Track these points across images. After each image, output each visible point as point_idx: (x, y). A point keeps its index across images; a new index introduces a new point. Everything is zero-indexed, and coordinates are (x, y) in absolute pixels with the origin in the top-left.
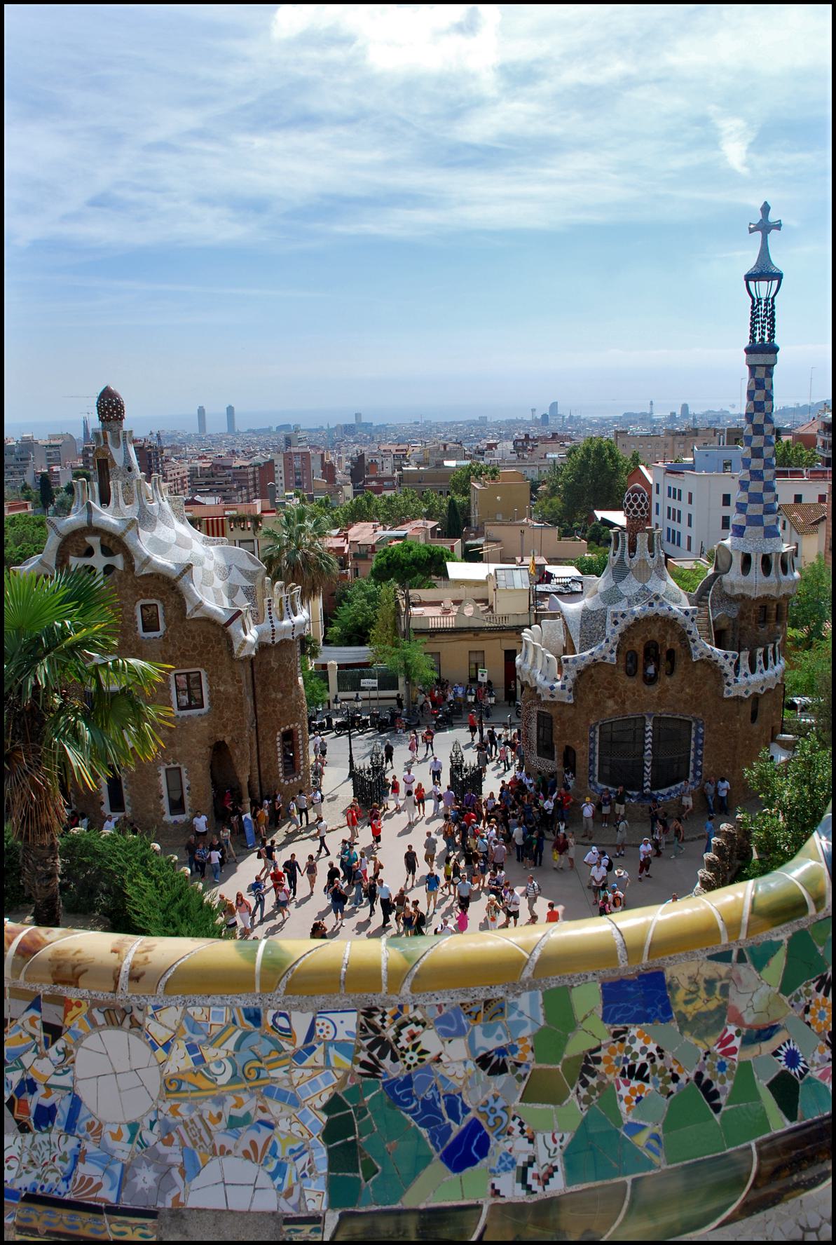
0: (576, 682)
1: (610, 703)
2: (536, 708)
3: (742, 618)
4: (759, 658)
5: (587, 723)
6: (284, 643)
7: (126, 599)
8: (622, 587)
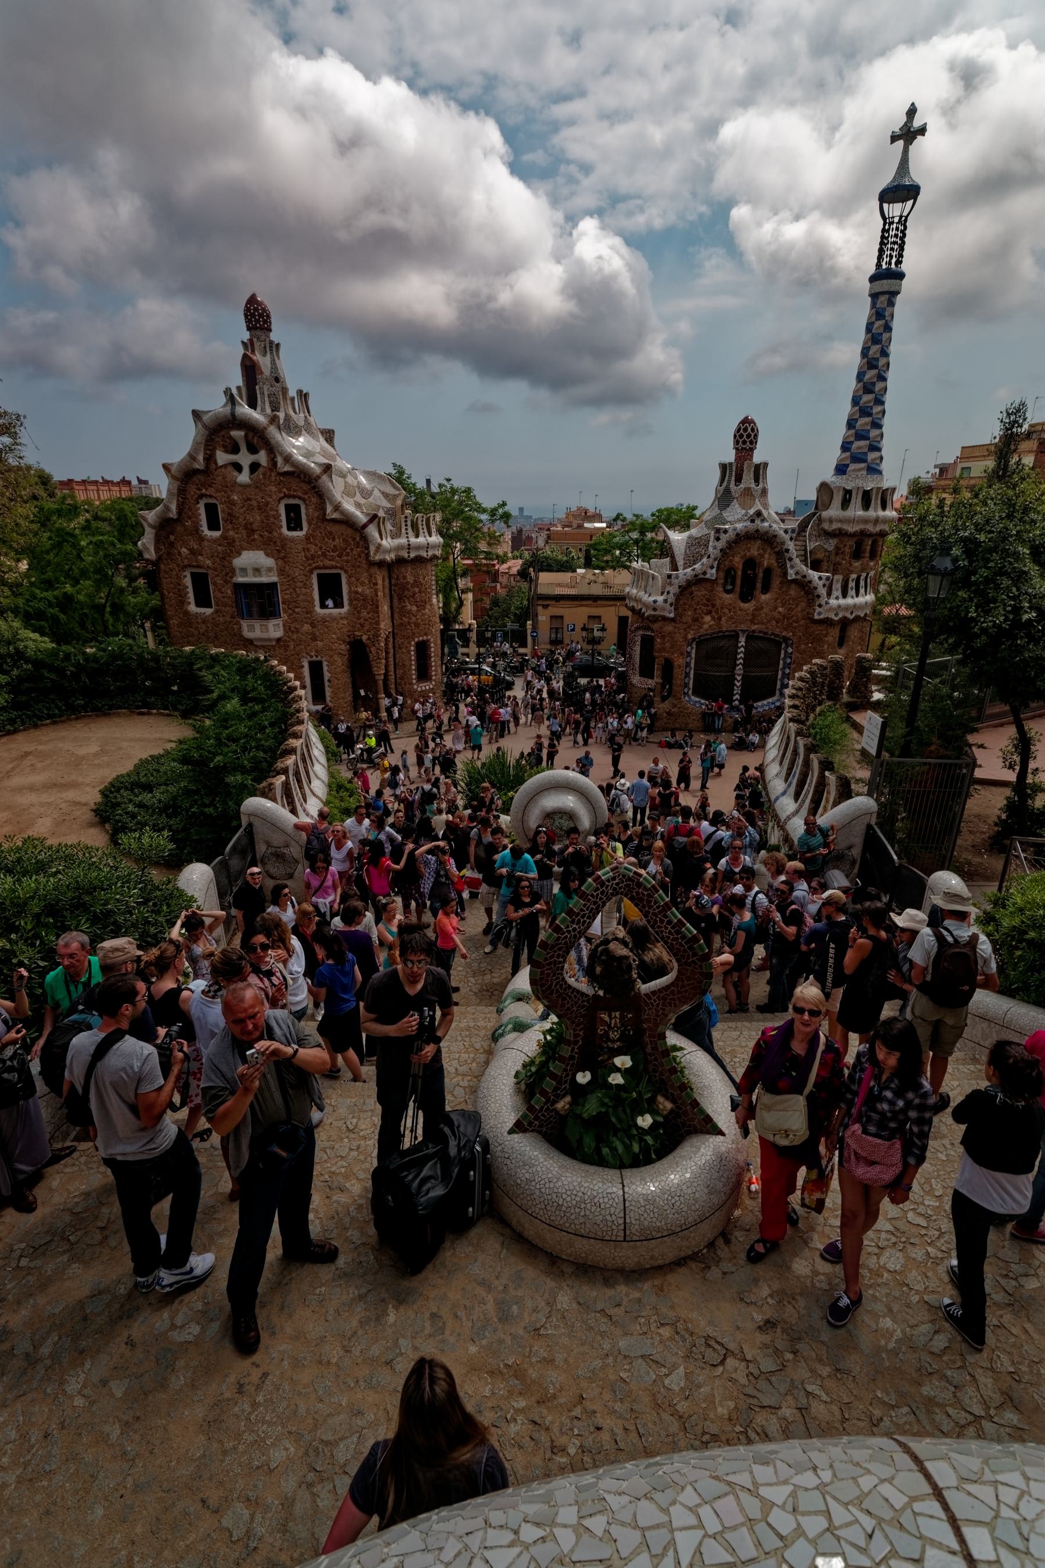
0: (678, 597)
1: (708, 618)
2: (641, 632)
3: (837, 554)
4: (852, 584)
5: (685, 637)
6: (419, 560)
7: (270, 496)
8: (725, 514)
